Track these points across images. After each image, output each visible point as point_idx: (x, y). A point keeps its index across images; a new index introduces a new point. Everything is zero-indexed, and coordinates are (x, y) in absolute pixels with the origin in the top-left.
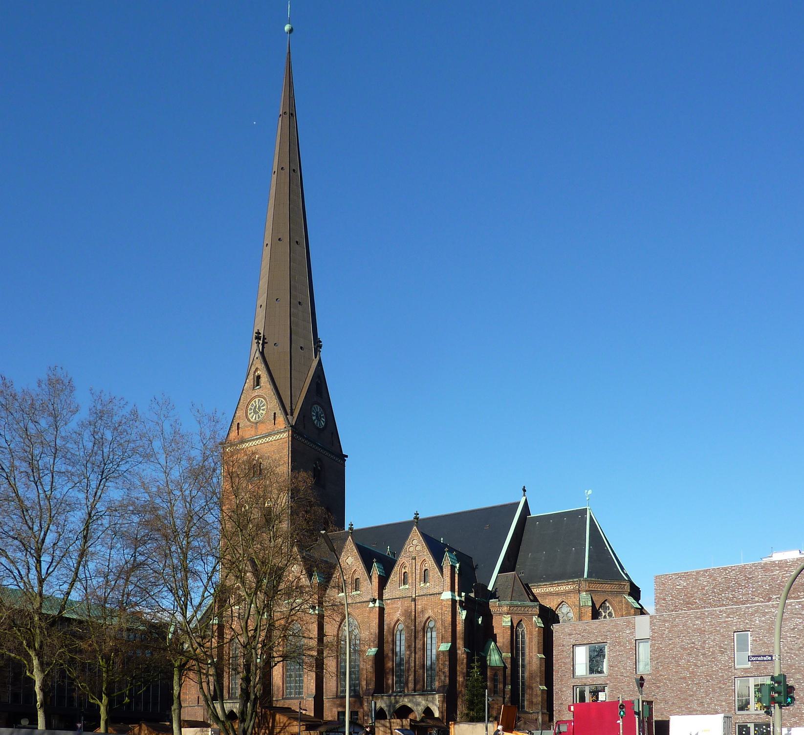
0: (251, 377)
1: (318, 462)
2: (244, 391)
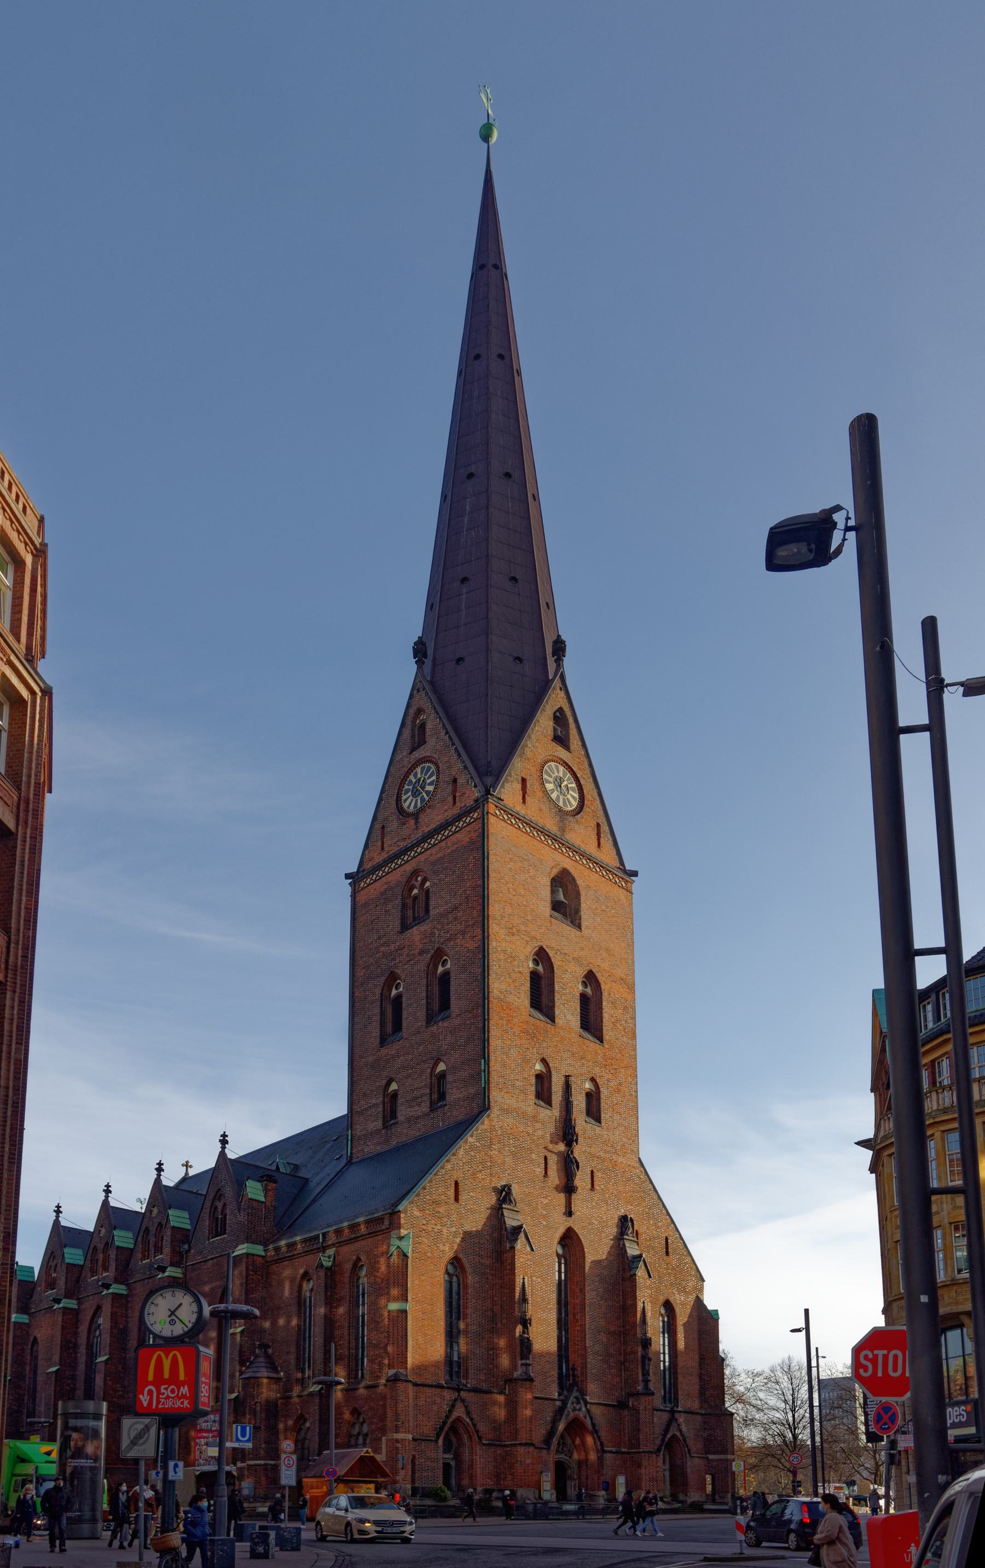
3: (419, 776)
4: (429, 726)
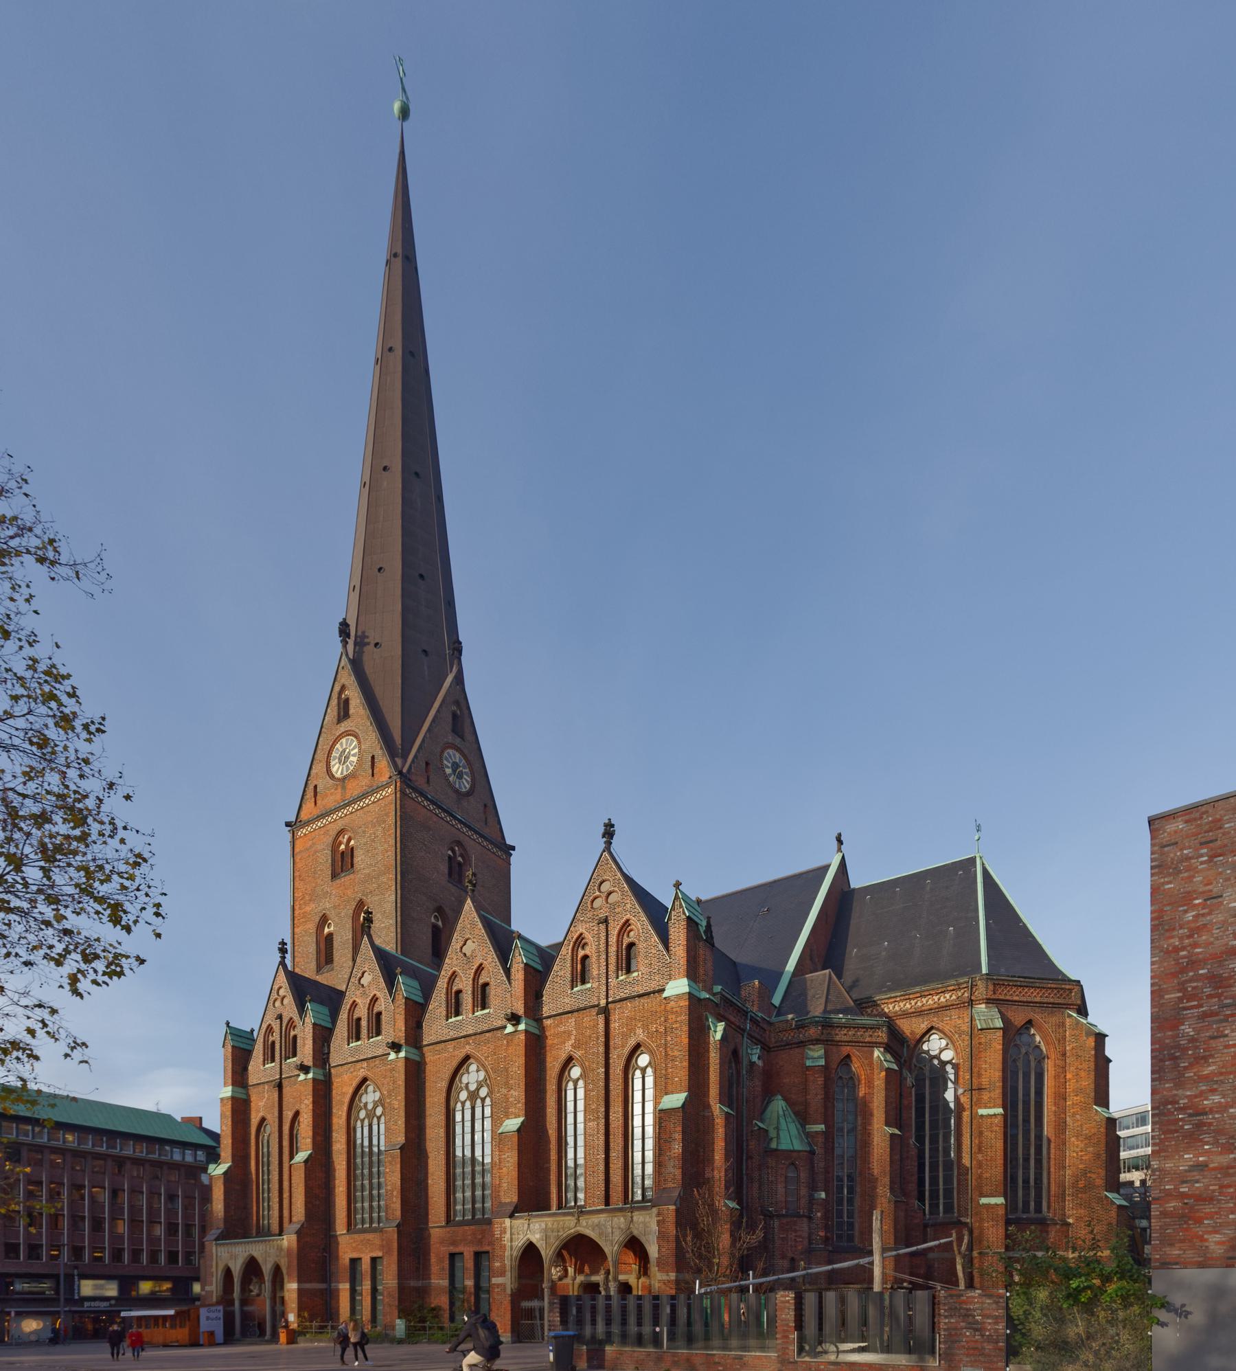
0: (334, 702)
1: (457, 848)
2: (323, 730)
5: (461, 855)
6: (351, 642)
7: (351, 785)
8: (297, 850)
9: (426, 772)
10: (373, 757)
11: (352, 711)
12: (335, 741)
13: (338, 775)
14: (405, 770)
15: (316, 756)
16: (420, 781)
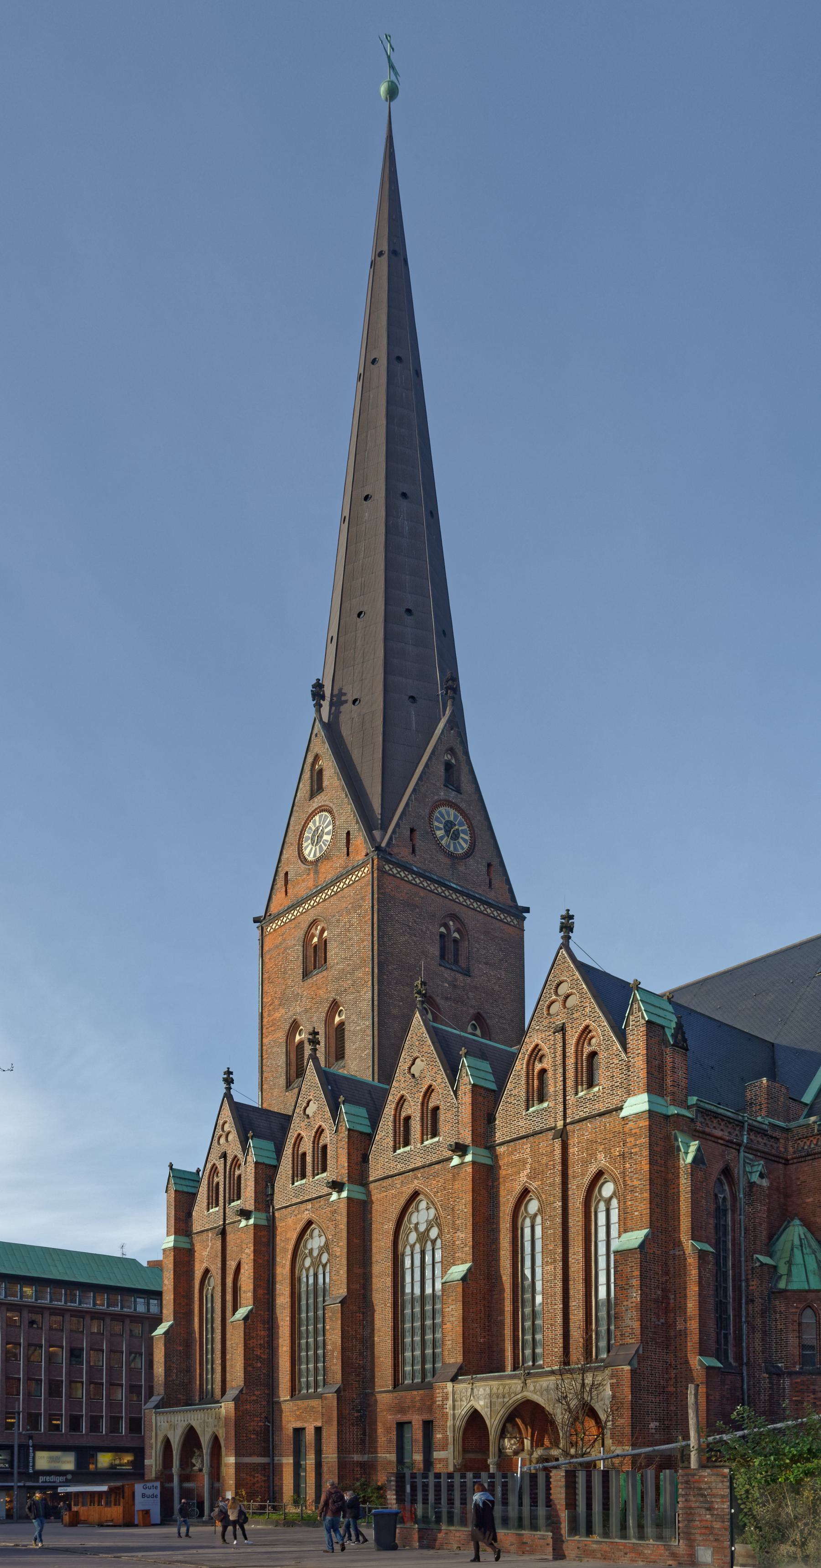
0: (307, 775)
1: (451, 923)
2: (295, 808)
3: (317, 824)
4: (327, 775)
5: (458, 930)
6: (326, 704)
7: (324, 868)
8: (266, 948)
9: (411, 840)
10: (348, 833)
11: (325, 783)
12: (307, 819)
13: (311, 858)
14: (383, 845)
15: (287, 839)
16: (403, 853)
